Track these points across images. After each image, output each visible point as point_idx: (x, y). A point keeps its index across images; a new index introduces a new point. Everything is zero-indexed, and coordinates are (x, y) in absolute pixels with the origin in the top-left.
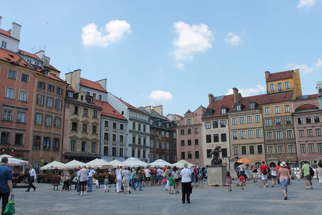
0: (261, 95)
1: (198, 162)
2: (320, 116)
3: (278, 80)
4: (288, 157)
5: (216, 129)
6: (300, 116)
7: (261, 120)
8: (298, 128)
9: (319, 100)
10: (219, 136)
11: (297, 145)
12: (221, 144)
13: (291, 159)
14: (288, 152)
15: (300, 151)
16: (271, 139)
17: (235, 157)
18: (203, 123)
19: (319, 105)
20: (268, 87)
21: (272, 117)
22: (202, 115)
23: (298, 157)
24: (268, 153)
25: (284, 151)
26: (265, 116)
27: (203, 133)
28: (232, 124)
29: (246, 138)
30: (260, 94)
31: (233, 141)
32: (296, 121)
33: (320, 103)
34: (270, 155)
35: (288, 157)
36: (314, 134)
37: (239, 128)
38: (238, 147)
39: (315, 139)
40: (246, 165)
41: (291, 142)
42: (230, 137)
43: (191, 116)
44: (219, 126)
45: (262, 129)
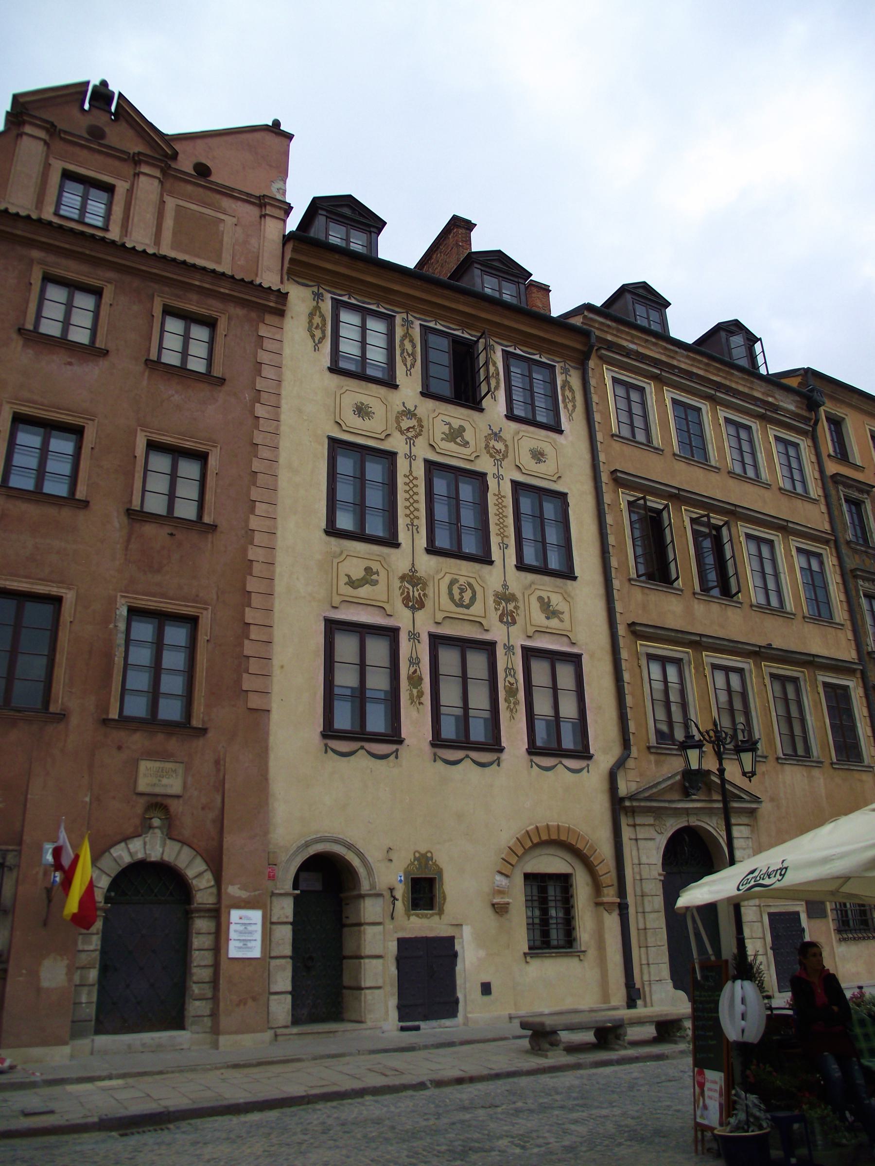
1: (173, 784)
5: (457, 415)
10: (491, 499)
18: (300, 298)
31: (638, 595)
38: (678, 662)
42: (611, 540)
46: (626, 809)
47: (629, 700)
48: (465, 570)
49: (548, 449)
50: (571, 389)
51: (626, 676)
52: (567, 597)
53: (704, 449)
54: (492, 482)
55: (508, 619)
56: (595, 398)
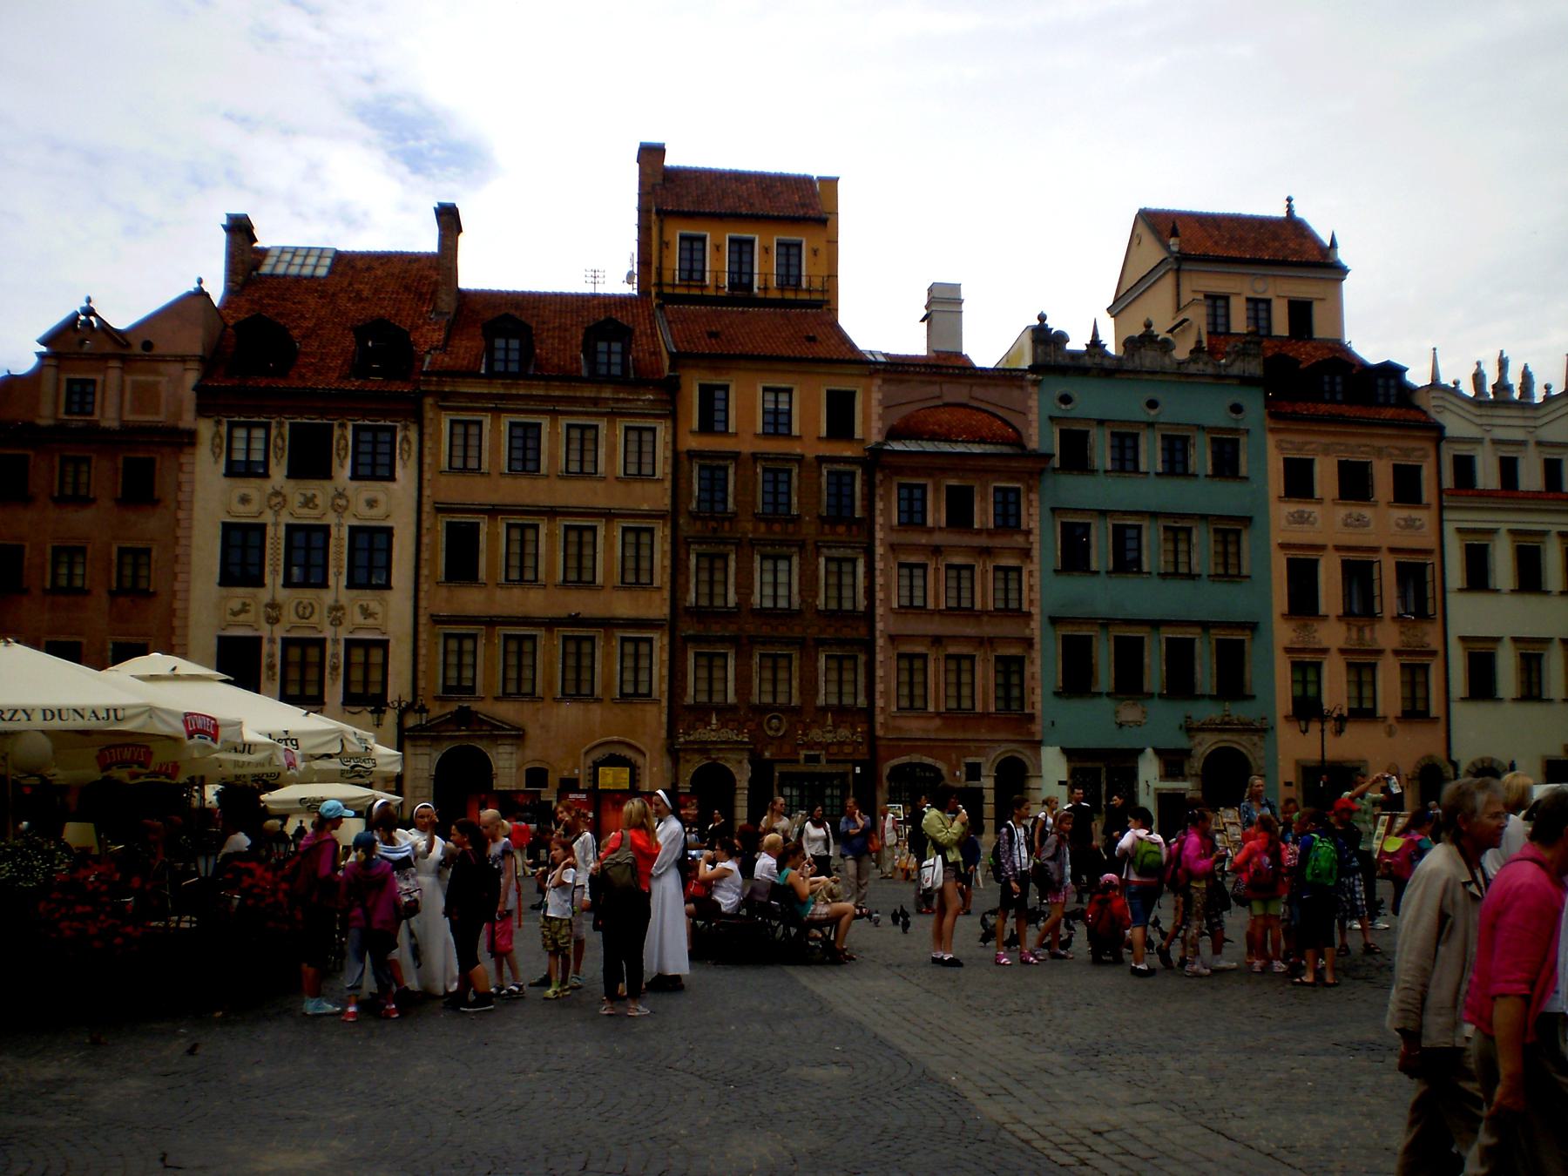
0: (595, 296)
2: (1030, 490)
3: (736, 217)
4: (816, 734)
6: (915, 472)
7: (659, 466)
8: (893, 548)
9: (1030, 389)
10: (332, 542)
11: (879, 657)
12: (344, 600)
13: (834, 749)
14: (821, 701)
15: (894, 694)
16: (718, 602)
17: (453, 707)
18: (206, 429)
19: (1029, 423)
20: (665, 252)
21: (735, 456)
22: (202, 359)
23: (880, 732)
24: (689, 700)
25: (795, 692)
26: (692, 443)
27: (197, 506)
28: (444, 464)
29: (542, 576)
30: (587, 289)
31: (443, 592)
32: (886, 498)
33: (1035, 410)
34: (701, 712)
35: (816, 734)
36: (984, 595)
37: (495, 499)
38: (474, 637)
39: (988, 629)
40: (529, 772)
41: (848, 633)
42: (425, 555)
43: (105, 357)
44: (343, 471)
45: (662, 533)
46: (409, 737)
47: (422, 667)
48: (307, 595)
49: (381, 497)
50: (409, 442)
51: (423, 651)
52: (383, 602)
53: (538, 461)
54: (334, 531)
55: (336, 622)
56: (428, 444)
